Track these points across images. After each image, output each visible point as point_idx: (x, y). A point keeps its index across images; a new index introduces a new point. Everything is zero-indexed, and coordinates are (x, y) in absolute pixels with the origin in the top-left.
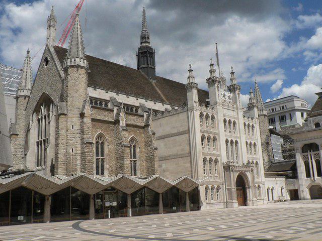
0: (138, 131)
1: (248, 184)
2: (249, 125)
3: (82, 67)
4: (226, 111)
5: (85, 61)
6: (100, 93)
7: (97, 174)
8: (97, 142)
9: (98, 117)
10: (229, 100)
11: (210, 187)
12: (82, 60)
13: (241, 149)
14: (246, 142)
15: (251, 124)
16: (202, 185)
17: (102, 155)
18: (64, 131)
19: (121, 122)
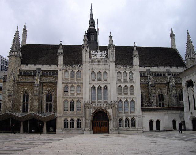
1: (110, 117)
3: (13, 56)
4: (95, 66)
5: (16, 53)
6: (30, 67)
7: (23, 111)
8: (24, 95)
9: (25, 80)
10: (102, 57)
11: (69, 119)
12: (14, 52)
14: (120, 86)
15: (128, 72)
17: (28, 101)
18: (5, 90)
19: (36, 82)
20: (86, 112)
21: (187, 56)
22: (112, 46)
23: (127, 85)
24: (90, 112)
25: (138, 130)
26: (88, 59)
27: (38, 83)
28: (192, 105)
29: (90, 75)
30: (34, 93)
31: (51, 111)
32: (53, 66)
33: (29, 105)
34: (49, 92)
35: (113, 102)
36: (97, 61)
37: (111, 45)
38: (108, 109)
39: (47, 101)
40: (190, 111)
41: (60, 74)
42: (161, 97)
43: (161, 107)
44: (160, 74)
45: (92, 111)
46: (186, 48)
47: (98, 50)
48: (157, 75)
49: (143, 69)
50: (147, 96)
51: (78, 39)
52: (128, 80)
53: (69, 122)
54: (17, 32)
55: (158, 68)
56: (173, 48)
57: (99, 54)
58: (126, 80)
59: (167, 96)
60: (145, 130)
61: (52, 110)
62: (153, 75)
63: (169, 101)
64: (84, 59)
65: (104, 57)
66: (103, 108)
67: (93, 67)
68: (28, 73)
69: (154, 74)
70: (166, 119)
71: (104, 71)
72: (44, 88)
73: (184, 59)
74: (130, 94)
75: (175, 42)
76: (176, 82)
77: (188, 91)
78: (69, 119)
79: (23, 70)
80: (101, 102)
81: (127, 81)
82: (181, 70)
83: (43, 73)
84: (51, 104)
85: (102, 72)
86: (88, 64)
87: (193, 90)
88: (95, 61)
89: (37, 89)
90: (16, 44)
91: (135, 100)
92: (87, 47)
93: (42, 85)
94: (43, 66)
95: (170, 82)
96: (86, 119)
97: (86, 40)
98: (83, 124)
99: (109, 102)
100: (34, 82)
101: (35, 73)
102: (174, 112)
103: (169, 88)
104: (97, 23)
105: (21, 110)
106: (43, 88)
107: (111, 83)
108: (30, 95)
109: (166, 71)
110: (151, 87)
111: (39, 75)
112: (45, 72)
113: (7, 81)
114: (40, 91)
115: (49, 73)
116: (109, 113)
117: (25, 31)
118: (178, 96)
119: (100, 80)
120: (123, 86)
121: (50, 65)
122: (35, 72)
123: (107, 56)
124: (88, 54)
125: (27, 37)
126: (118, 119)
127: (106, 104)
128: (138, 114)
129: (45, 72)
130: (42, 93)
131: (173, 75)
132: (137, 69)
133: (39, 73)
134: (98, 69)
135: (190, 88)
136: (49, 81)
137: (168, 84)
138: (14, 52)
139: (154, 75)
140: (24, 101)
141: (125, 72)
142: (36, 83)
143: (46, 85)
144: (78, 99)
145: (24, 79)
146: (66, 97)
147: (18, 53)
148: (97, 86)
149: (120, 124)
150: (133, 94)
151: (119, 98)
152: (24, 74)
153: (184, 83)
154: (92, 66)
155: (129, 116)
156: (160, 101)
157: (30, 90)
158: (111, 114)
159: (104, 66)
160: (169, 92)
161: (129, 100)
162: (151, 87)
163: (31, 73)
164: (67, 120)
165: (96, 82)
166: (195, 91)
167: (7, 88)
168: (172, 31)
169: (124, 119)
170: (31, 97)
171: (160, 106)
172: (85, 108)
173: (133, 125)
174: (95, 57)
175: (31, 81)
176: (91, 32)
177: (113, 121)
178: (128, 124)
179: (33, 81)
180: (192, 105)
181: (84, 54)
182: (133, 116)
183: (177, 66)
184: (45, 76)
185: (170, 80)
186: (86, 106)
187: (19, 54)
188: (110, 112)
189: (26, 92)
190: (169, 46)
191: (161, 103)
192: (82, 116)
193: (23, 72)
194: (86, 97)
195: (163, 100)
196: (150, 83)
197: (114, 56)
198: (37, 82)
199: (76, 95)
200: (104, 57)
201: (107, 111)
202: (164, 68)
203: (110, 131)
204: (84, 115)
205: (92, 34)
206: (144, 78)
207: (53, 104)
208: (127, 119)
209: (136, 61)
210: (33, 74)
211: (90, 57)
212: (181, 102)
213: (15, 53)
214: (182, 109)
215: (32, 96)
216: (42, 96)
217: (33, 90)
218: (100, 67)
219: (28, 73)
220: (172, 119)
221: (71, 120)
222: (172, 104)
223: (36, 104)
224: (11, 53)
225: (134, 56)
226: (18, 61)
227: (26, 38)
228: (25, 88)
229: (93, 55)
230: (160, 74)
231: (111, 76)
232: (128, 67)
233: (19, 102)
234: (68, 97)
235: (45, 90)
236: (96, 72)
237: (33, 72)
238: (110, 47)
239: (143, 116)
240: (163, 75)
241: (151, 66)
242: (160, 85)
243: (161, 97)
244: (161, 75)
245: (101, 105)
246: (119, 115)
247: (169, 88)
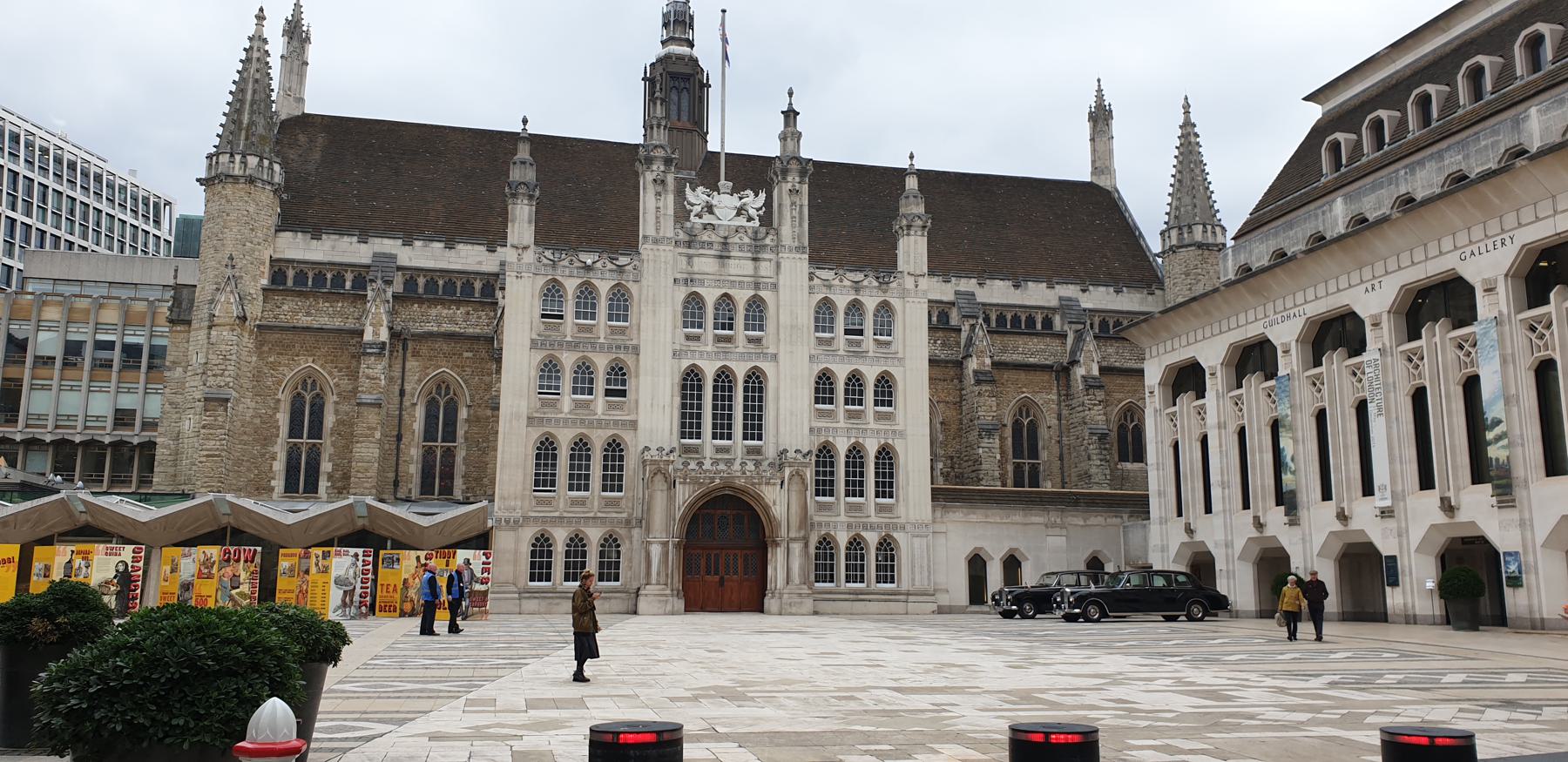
0: (466, 354)
2: (855, 307)
3: (235, 178)
4: (705, 264)
5: (253, 161)
6: (333, 248)
7: (291, 487)
9: (304, 321)
11: (560, 537)
12: (238, 158)
13: (777, 399)
15: (870, 303)
16: (515, 525)
17: (316, 431)
18: (180, 369)
20: (651, 496)
21: (1174, 233)
22: (794, 166)
23: (863, 369)
24: (671, 499)
25: (911, 598)
26: (668, 229)
27: (384, 336)
28: (1193, 489)
29: (679, 308)
30: (355, 391)
31: (447, 490)
32: (469, 247)
33: (325, 457)
34: (442, 385)
35: (791, 454)
36: (714, 238)
37: (791, 162)
38: (763, 487)
39: (429, 434)
40: (1180, 514)
41: (521, 304)
42: (1025, 438)
43: (1025, 489)
44: (1023, 319)
45: (684, 495)
46: (1171, 190)
47: (724, 184)
48: (1010, 323)
49: (944, 291)
50: (954, 427)
51: (618, 117)
53: (559, 549)
54: (258, 40)
55: (1016, 286)
56: (1102, 182)
57: (726, 203)
58: (859, 343)
59: (1054, 433)
60: (944, 600)
61: (459, 485)
62: (987, 320)
63: (1066, 456)
64: (647, 227)
65: (750, 219)
66: (741, 482)
68: (320, 279)
69: (993, 317)
70: (1050, 549)
71: (752, 293)
72: (412, 364)
73: (1155, 245)
74: (879, 417)
75: (1110, 152)
76: (1104, 364)
77: (1174, 414)
78: (560, 537)
79: (293, 261)
81: (864, 347)
82: (1129, 301)
83: (406, 283)
84: (449, 454)
85: (742, 296)
86: (667, 253)
87: (1201, 411)
88: (705, 238)
89: (375, 370)
90: (252, 112)
91: (899, 446)
92: (668, 161)
93: (405, 349)
94: (407, 243)
95: (1074, 362)
96: (648, 531)
97: (659, 126)
98: (630, 560)
99: (770, 452)
100: (361, 333)
101: (361, 283)
102: (1097, 520)
103: (1066, 394)
104: (725, 41)
105: (278, 484)
106: (408, 365)
107: (781, 357)
108: (331, 400)
109: (1054, 303)
110: (978, 382)
111: (389, 294)
112: (421, 281)
113: (200, 315)
114: (391, 379)
115: (441, 283)
116: (766, 509)
117: (296, 32)
118: (1114, 435)
119: (729, 339)
120: (841, 373)
121: (450, 246)
122: (362, 276)
123: (767, 219)
124: (671, 198)
125: (310, 70)
126: (814, 540)
127: (757, 464)
128: (912, 519)
129: (421, 281)
130: (402, 393)
131: (1092, 325)
132: (915, 287)
133: (389, 283)
134: (718, 283)
135: (1186, 401)
136: (447, 327)
137: (1063, 372)
138: (238, 158)
139: (993, 324)
140: (295, 430)
141: (855, 307)
142: (368, 336)
143: (424, 350)
144: (611, 432)
145: (295, 313)
146: (549, 420)
147: (266, 163)
148: (709, 369)
149: (823, 567)
150: (888, 417)
151: (819, 429)
152: (295, 283)
153: (1154, 373)
155: (865, 528)
156: (1017, 453)
157: (330, 373)
158: (779, 511)
159: (748, 267)
160: (1065, 412)
161: (871, 447)
162: (978, 382)
163: (339, 280)
164: (547, 540)
166: (1212, 418)
167: (197, 360)
168: (1100, 90)
169: (843, 539)
170: (337, 412)
171: (1018, 482)
172: (648, 484)
173: (887, 571)
174: (707, 218)
175: (337, 323)
176: (674, 76)
178: (859, 572)
179: (350, 324)
180: (1193, 489)
181: (649, 202)
182: (887, 525)
183: (1117, 283)
184: (420, 301)
185: (1073, 352)
186: (658, 470)
187: (271, 168)
188: (778, 501)
189: (308, 381)
190: (1083, 174)
191: (1027, 468)
192: (628, 521)
193: (291, 273)
194: (654, 417)
195: (1034, 453)
196: (973, 365)
197: (801, 219)
198: (376, 333)
199: (600, 410)
200: (750, 219)
201: (759, 498)
202: (1050, 287)
203: (770, 603)
204: (638, 513)
205: (677, 86)
206: (940, 334)
207: (460, 455)
208: (856, 544)
209: (913, 249)
210: (348, 285)
211: (682, 214)
212: (1129, 466)
213: (244, 163)
214: (1139, 506)
215: (345, 408)
216: (401, 409)
217: (354, 375)
218: (732, 271)
219: (320, 279)
220: (1085, 555)
221: (537, 539)
222: (1086, 476)
223: (367, 452)
224: (224, 159)
225: (904, 222)
226: (264, 206)
227: (301, 76)
228: (306, 363)
229: (697, 209)
230: (1023, 319)
231: (785, 319)
233: (268, 440)
234: (558, 421)
235: (418, 375)
236: (710, 295)
237: (349, 277)
238: (785, 172)
239: (938, 527)
240: (1039, 326)
241: (985, 274)
242: (1022, 376)
243: (1025, 438)
244: (1031, 321)
245: (729, 462)
246: (817, 519)
247: (1066, 394)
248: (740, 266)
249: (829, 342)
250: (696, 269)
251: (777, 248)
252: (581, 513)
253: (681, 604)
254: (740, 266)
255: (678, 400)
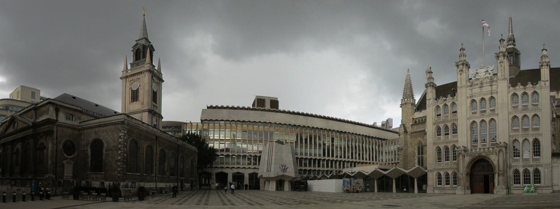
38: (491, 155)
52: (530, 106)
53: (443, 177)
67: (473, 92)
71: (490, 96)
80: (485, 145)
85: (487, 97)
119: (485, 111)
148: (478, 121)
154: (472, 91)
165: (478, 115)
177: (499, 175)
203: (495, 191)
218: (484, 91)
232: (529, 85)
236: (478, 99)
246: (513, 164)
248: (487, 88)
249: (517, 107)
250: (473, 92)
251: (496, 81)
252: (447, 166)
253: (469, 191)
254: (487, 88)
255: (469, 132)
